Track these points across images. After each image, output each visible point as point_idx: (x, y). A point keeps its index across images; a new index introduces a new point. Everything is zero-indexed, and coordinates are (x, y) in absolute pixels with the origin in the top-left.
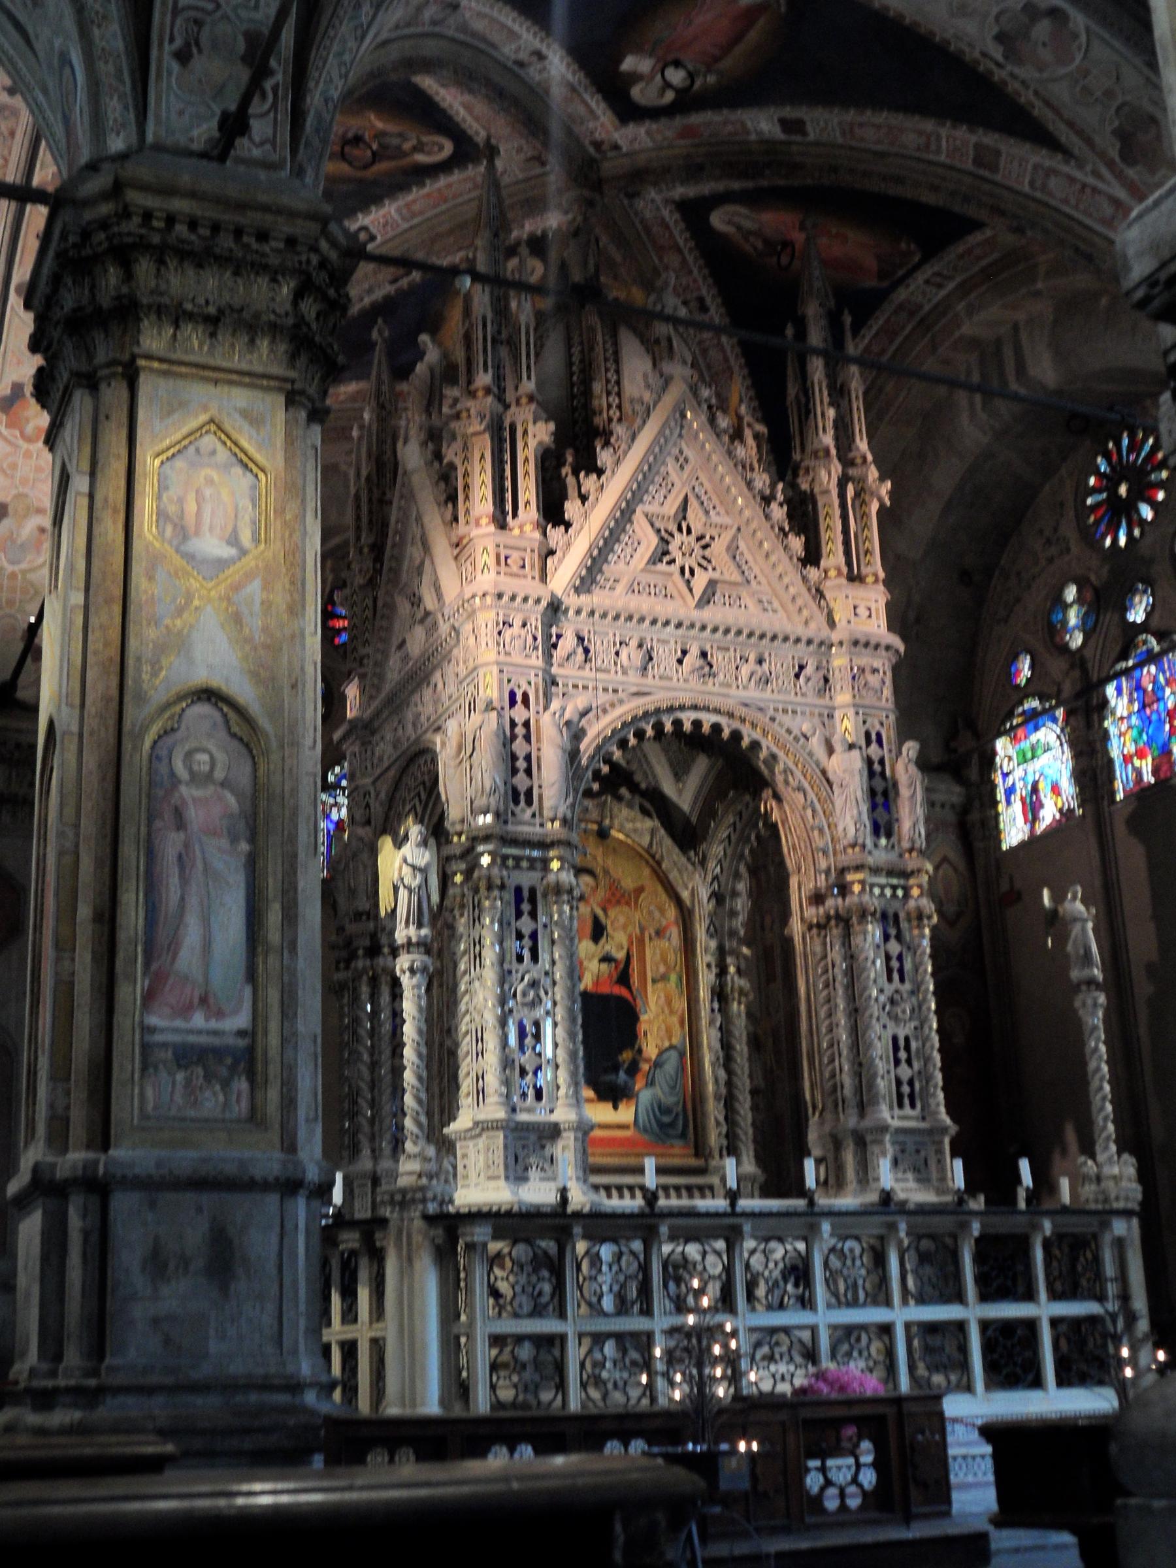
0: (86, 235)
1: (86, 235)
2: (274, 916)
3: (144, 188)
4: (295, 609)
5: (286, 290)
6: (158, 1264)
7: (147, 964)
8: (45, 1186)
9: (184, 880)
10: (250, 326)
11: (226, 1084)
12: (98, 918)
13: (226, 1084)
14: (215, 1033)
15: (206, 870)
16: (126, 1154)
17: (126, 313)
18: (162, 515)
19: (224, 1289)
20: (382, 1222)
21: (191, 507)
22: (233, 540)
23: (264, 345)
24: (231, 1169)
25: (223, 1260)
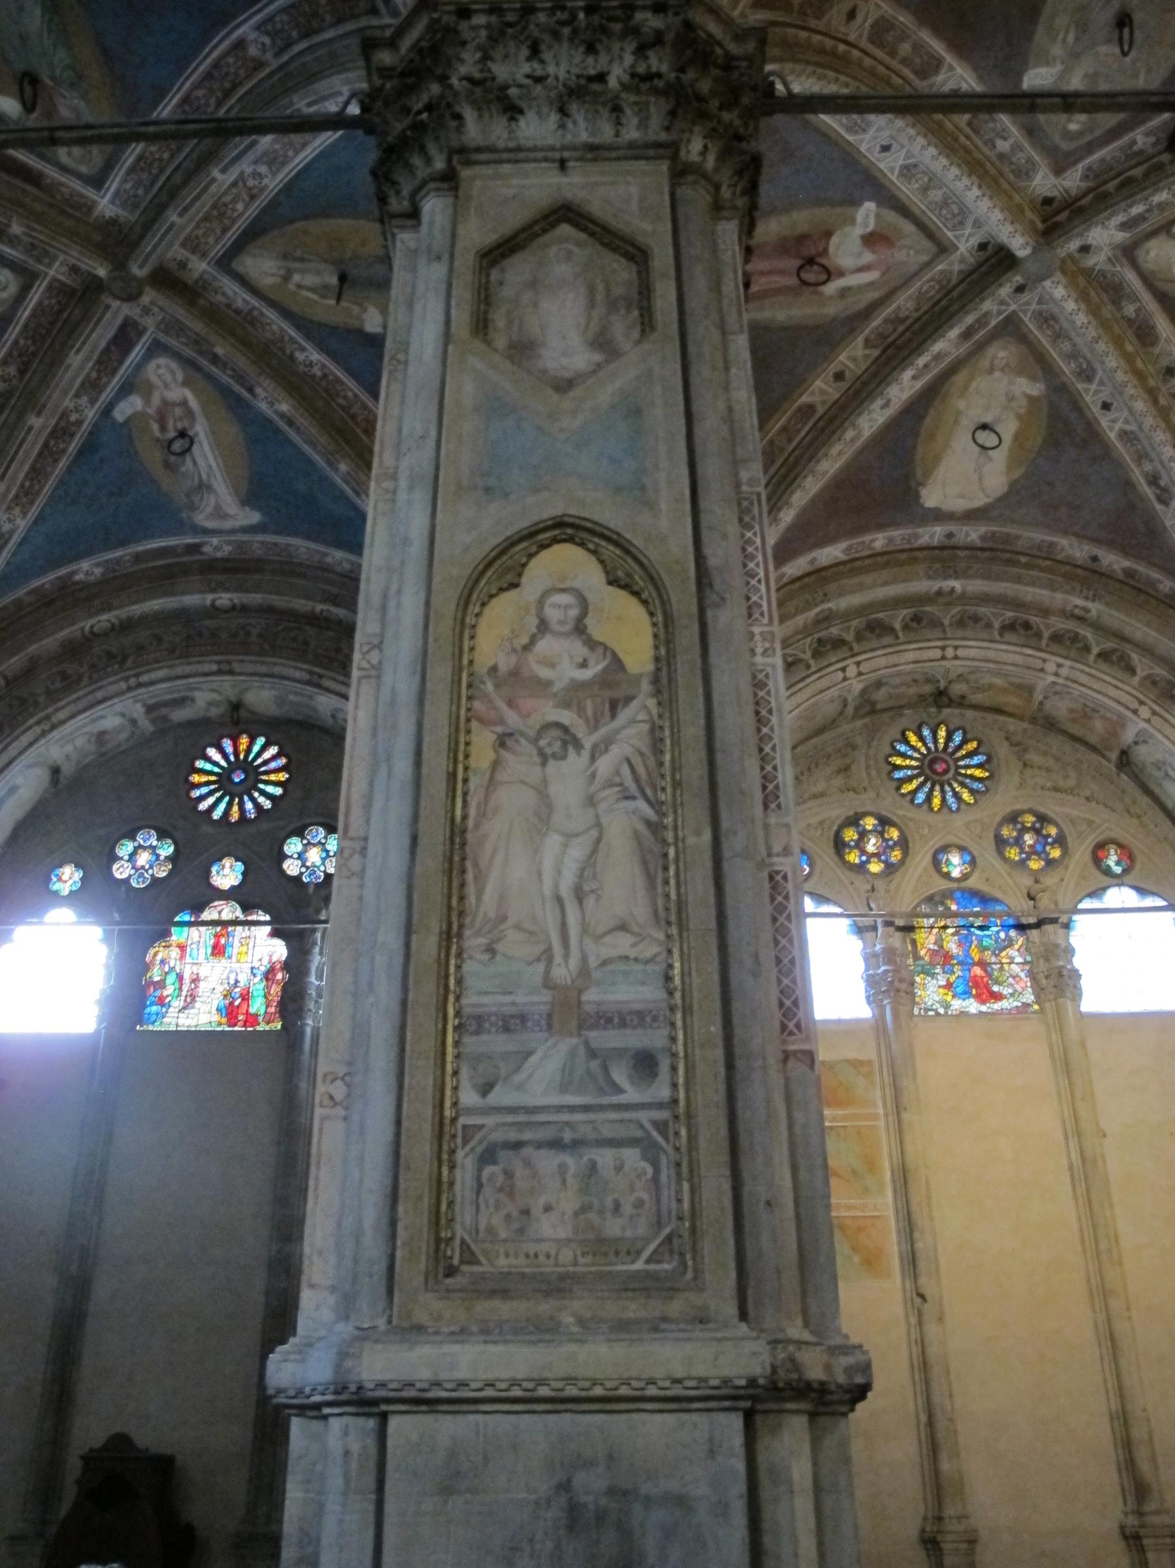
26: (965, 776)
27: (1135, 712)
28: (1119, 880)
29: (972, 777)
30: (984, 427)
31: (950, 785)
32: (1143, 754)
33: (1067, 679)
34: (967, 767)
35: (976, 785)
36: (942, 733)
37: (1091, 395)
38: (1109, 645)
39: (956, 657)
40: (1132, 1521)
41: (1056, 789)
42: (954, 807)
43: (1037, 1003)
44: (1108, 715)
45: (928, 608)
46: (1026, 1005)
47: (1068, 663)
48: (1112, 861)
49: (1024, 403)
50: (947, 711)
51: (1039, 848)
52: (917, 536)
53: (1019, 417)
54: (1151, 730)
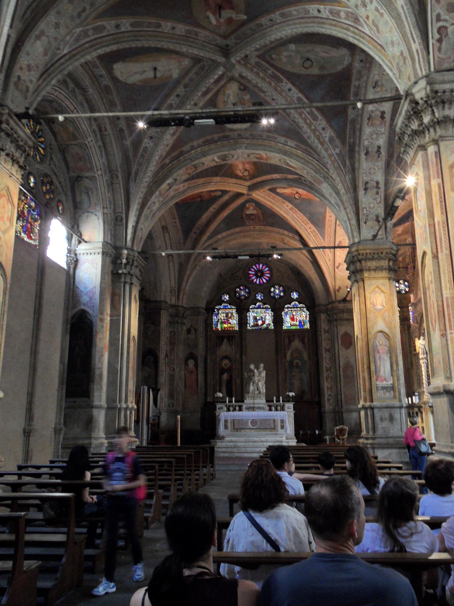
0: (353, 257)
1: (353, 257)
2: (395, 366)
3: (362, 250)
4: (394, 314)
5: (387, 262)
6: (382, 419)
8: (364, 408)
9: (380, 361)
11: (390, 392)
12: (368, 368)
16: (375, 403)
17: (361, 271)
18: (371, 303)
19: (392, 423)
20: (422, 407)
21: (375, 301)
22: (382, 305)
23: (384, 272)
24: (391, 405)
25: (391, 419)
27: (97, 170)
32: (87, 182)
37: (180, 90)
40: (27, 428)
43: (39, 246)
52: (97, 67)
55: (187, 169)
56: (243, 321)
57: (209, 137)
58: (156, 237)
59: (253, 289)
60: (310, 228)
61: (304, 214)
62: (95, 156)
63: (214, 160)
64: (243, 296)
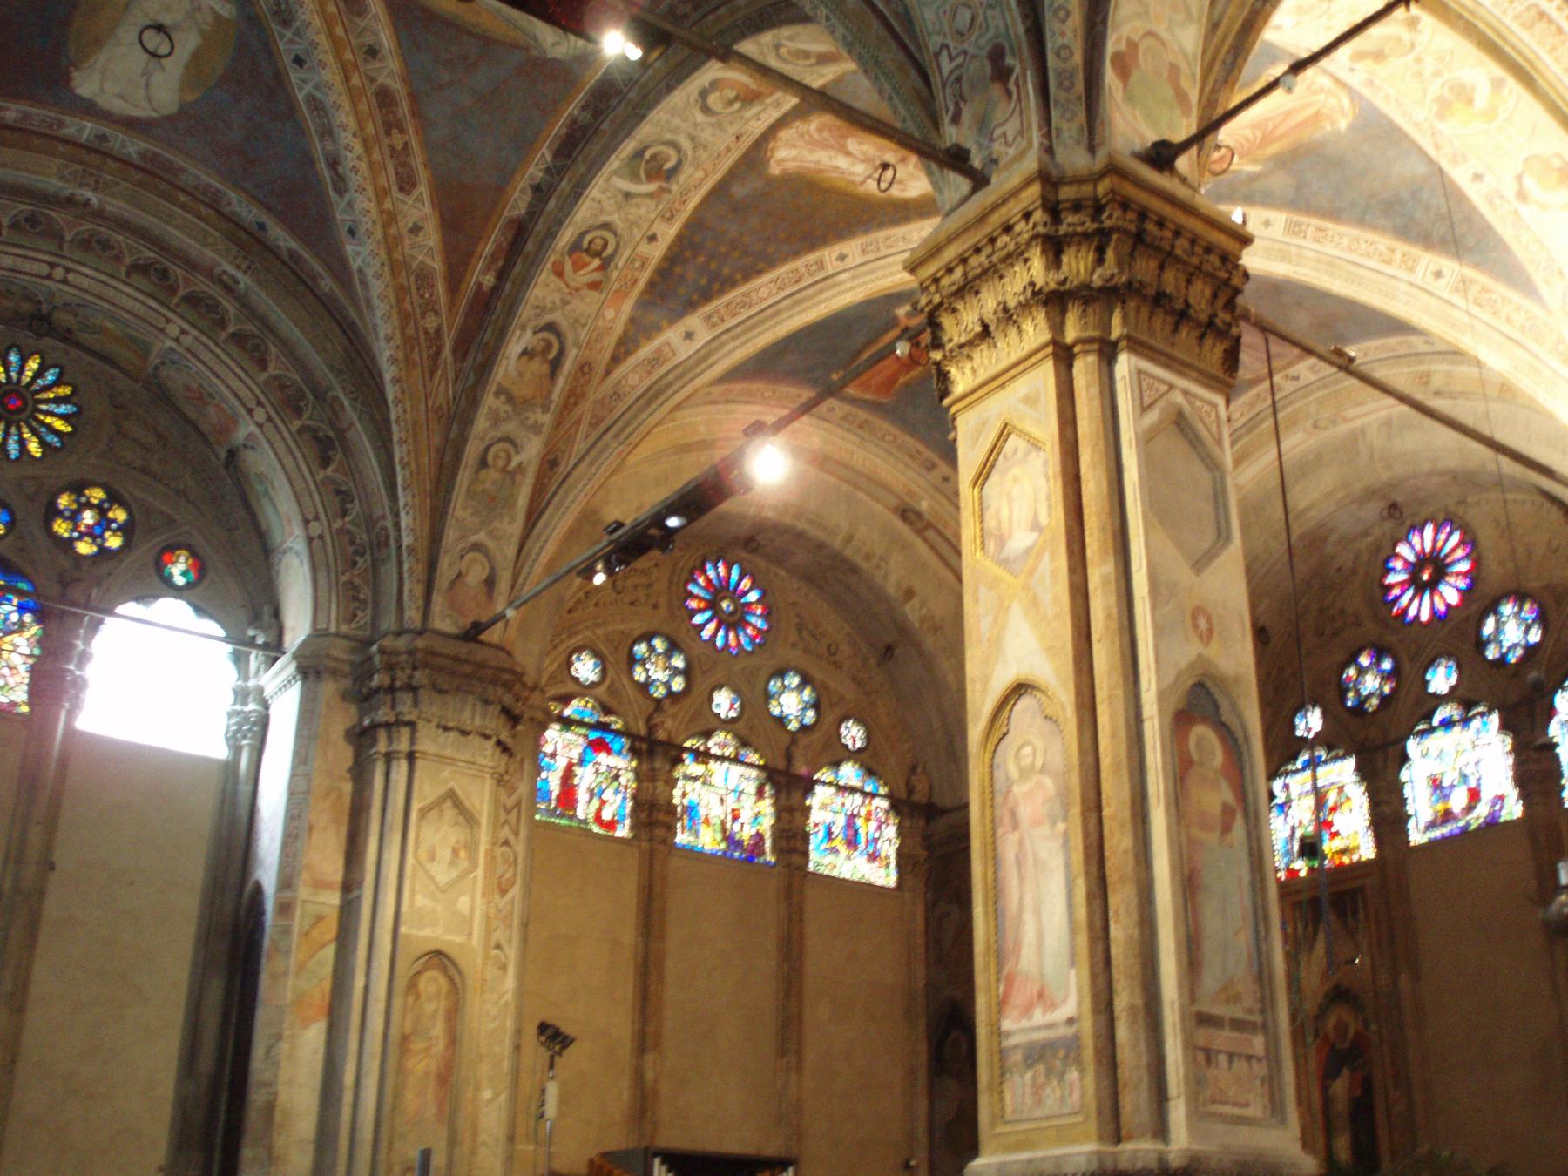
7: (999, 972)
9: (1022, 880)
10: (1008, 316)
13: (1062, 1075)
14: (1051, 1026)
15: (1035, 860)
21: (1005, 513)
22: (1036, 526)
23: (1028, 326)
26: (42, 423)
27: (250, 411)
28: (178, 592)
29: (50, 428)
30: (160, 28)
31: (19, 428)
33: (187, 349)
34: (51, 414)
35: (52, 439)
36: (33, 364)
38: (249, 327)
39: (65, 281)
41: (144, 470)
42: (14, 454)
44: (224, 405)
45: (52, 214)
46: (14, 704)
47: (195, 332)
48: (178, 570)
49: (210, 19)
50: (48, 342)
51: (98, 530)
52: (62, 125)
53: (202, 33)
54: (261, 437)
55: (559, 273)
56: (1388, 815)
57: (559, 127)
58: (868, 557)
59: (1410, 649)
60: (1438, 274)
61: (1361, 222)
62: (220, 370)
63: (628, 195)
64: (1371, 695)
